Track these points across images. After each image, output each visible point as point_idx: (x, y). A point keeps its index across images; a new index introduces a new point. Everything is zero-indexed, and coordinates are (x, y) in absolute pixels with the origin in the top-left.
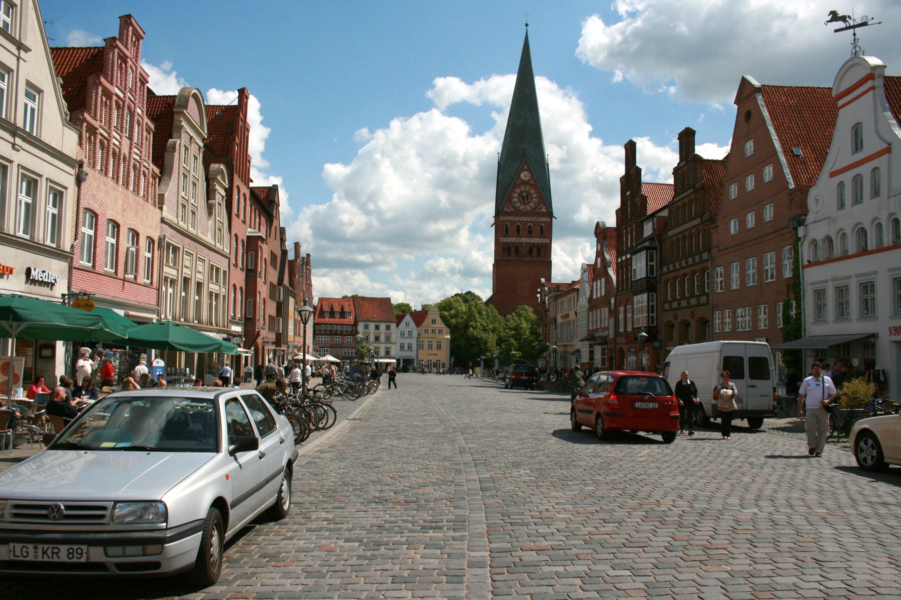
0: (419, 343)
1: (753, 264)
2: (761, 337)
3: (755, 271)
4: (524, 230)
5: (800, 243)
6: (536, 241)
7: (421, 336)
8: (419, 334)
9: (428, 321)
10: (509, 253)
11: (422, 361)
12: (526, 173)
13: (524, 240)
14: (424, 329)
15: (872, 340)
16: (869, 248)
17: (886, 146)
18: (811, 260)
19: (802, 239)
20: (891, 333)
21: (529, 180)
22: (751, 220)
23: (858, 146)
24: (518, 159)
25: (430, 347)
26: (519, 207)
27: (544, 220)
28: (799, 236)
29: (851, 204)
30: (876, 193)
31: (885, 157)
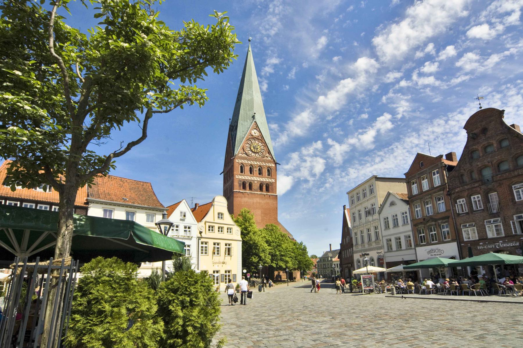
0: (200, 245)
4: (256, 171)
6: (265, 180)
7: (203, 235)
8: (201, 233)
9: (210, 217)
10: (244, 188)
11: (217, 272)
12: (255, 130)
13: (255, 179)
14: (208, 224)
21: (258, 137)
24: (248, 121)
25: (216, 251)
26: (251, 154)
27: (270, 165)
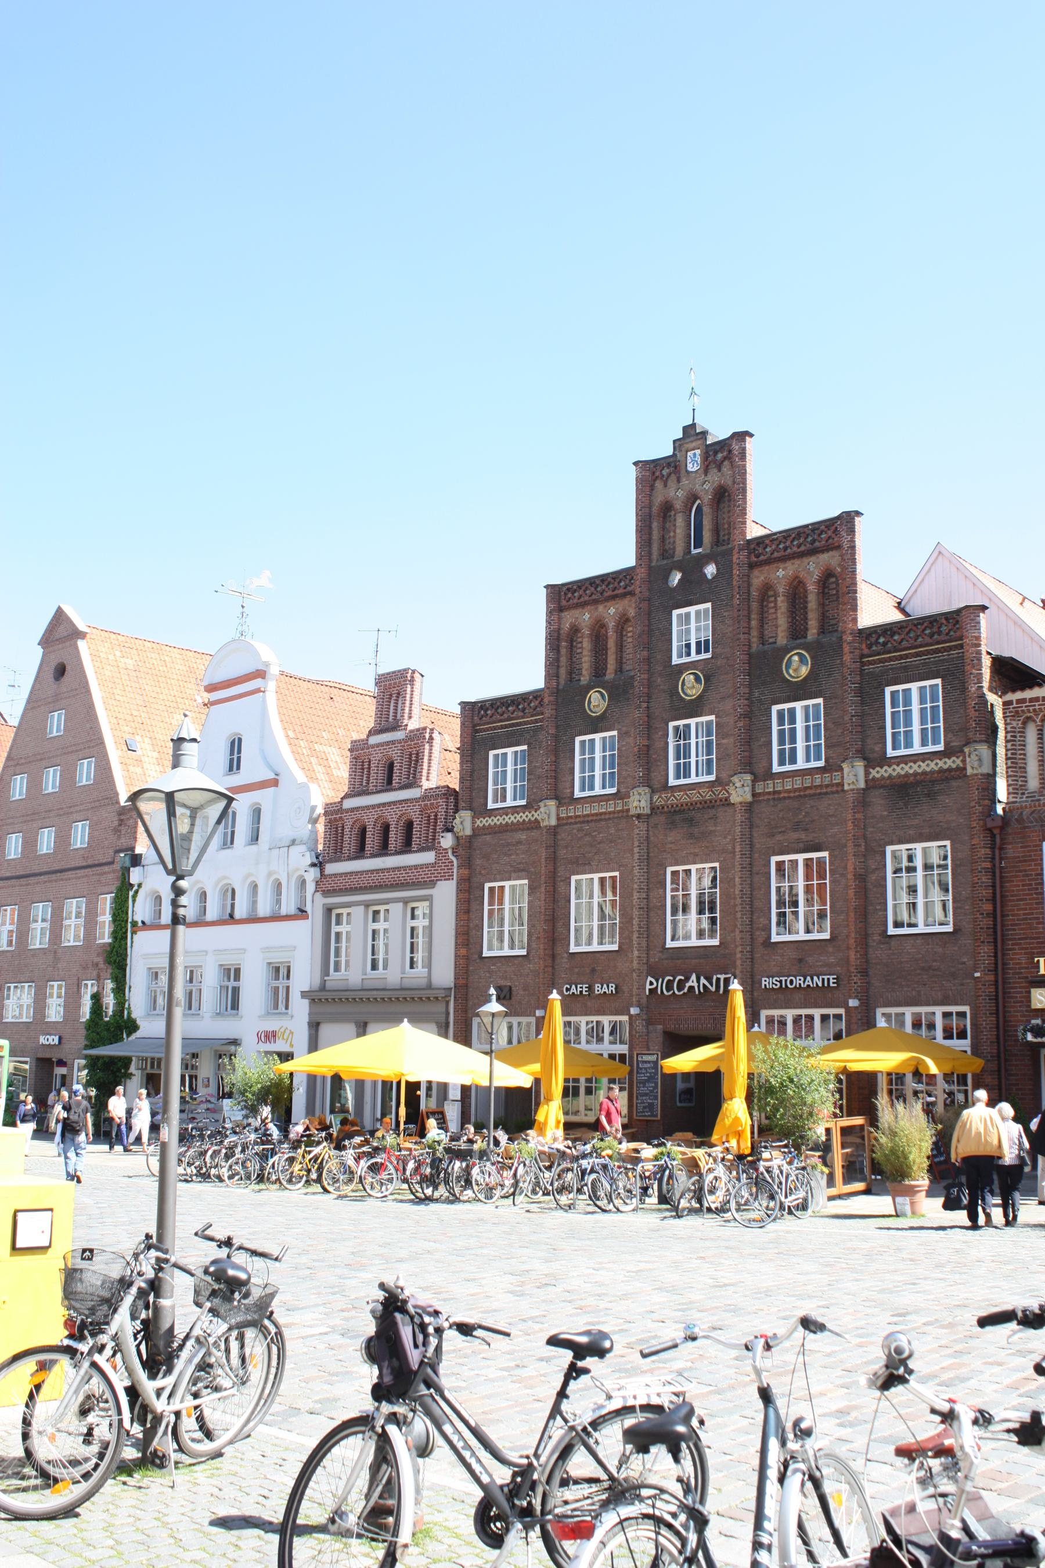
1: (44, 912)
2: (51, 1035)
3: (47, 925)
5: (131, 893)
15: (233, 1048)
16: (237, 915)
17: (273, 776)
18: (147, 921)
19: (135, 888)
20: (259, 1039)
22: (46, 841)
23: (234, 765)
28: (132, 882)
29: (216, 848)
30: (255, 838)
31: (271, 790)
